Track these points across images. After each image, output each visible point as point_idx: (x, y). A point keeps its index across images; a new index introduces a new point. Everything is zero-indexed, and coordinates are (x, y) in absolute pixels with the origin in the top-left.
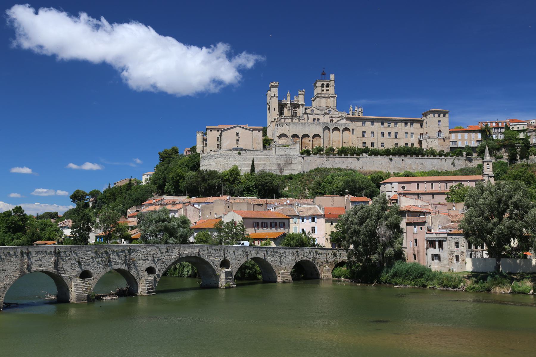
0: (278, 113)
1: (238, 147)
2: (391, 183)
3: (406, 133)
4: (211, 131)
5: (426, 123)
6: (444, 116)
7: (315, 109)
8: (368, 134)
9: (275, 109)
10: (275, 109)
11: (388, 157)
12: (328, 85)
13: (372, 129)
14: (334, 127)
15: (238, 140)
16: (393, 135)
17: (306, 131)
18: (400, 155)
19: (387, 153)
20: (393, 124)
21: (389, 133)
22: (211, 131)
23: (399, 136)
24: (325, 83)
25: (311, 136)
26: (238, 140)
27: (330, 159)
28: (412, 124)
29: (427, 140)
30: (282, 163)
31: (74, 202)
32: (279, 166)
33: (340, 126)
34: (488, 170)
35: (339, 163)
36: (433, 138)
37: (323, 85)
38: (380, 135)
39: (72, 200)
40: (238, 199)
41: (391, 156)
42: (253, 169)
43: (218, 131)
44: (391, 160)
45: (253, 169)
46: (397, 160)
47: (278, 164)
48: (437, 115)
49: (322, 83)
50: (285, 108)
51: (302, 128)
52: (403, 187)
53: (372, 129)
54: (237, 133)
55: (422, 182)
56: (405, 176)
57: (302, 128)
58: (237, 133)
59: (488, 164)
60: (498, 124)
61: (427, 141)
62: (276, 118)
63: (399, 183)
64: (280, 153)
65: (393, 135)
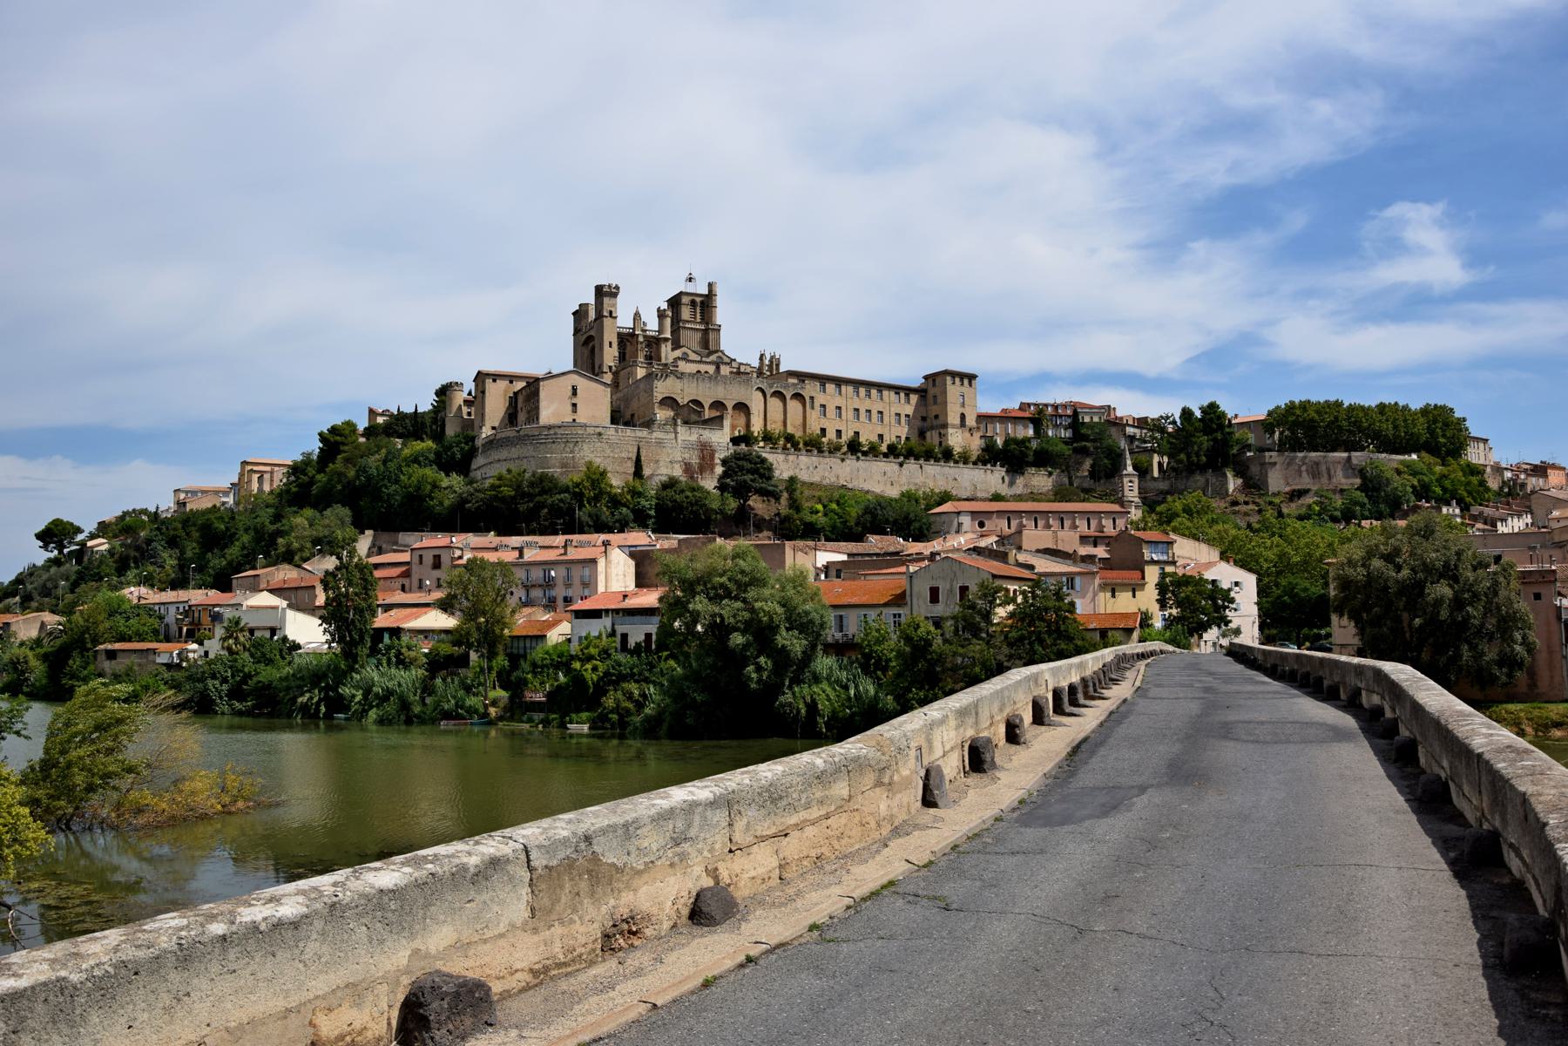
0: (617, 354)
1: (574, 420)
2: (959, 513)
3: (898, 415)
4: (494, 381)
5: (935, 397)
6: (970, 385)
7: (690, 352)
8: (831, 411)
9: (610, 343)
10: (610, 343)
11: (897, 461)
12: (702, 302)
13: (839, 401)
14: (772, 390)
15: (574, 405)
16: (875, 415)
17: (719, 392)
18: (917, 459)
19: (893, 451)
20: (874, 392)
21: (869, 411)
22: (494, 381)
23: (886, 419)
24: (698, 300)
25: (730, 405)
26: (574, 405)
27: (791, 458)
28: (907, 395)
29: (942, 432)
30: (695, 461)
31: (45, 547)
32: (688, 468)
33: (785, 388)
34: (1131, 494)
35: (808, 468)
36: (954, 426)
37: (693, 303)
38: (851, 414)
39: (41, 544)
40: (667, 539)
41: (901, 459)
42: (638, 472)
43: (511, 382)
44: (901, 465)
45: (638, 472)
46: (912, 466)
47: (686, 464)
48: (957, 380)
49: (691, 298)
50: (628, 344)
51: (710, 388)
52: (981, 525)
53: (839, 401)
54: (574, 392)
55: (1019, 513)
56: (991, 500)
57: (710, 388)
58: (574, 392)
59: (1131, 482)
60: (1056, 407)
61: (940, 434)
62: (612, 364)
63: (973, 513)
64: (690, 439)
65: (875, 415)
